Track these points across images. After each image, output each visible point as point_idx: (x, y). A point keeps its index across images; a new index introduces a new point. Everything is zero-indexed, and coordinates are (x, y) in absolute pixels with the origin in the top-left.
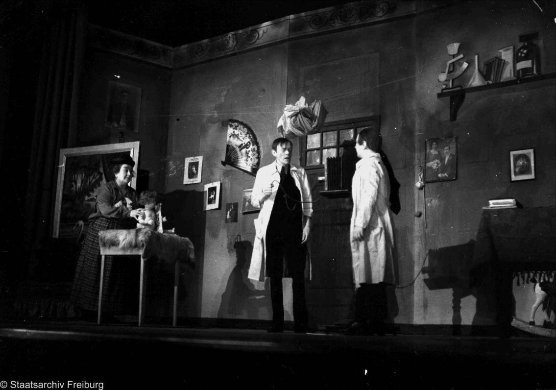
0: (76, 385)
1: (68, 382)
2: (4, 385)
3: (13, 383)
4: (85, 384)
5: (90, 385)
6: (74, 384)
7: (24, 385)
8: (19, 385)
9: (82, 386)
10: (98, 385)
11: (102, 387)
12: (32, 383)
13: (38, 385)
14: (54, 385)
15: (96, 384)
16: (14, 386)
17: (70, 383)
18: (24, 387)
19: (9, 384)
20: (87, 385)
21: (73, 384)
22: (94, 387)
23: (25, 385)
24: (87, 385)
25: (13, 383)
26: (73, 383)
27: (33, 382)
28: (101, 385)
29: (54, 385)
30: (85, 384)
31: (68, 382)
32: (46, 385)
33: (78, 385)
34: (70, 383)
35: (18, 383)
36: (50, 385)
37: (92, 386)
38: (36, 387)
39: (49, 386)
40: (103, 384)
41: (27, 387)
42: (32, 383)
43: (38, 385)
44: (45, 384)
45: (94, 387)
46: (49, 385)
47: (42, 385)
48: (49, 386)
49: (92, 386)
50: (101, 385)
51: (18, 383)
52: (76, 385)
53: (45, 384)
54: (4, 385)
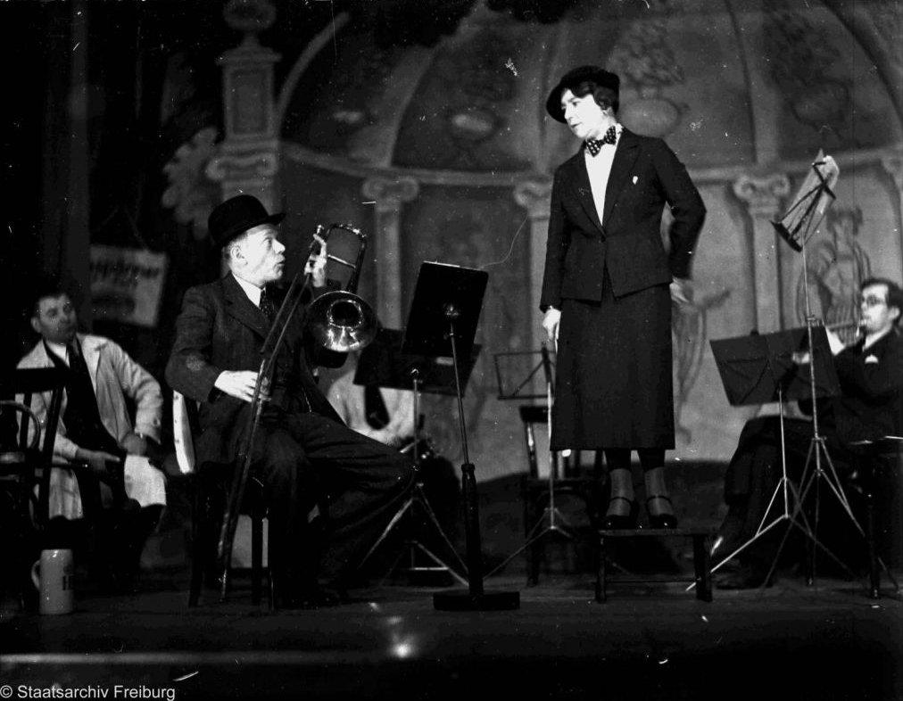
0: (128, 692)
3: (22, 689)
4: (144, 692)
5: (152, 693)
6: (126, 691)
8: (33, 693)
9: (138, 694)
10: (165, 692)
11: (173, 696)
12: (53, 689)
13: (64, 693)
14: (92, 692)
15: (163, 690)
16: (23, 694)
17: (118, 689)
19: (16, 691)
20: (147, 693)
21: (124, 691)
22: (158, 696)
23: (42, 693)
24: (147, 693)
25: (22, 689)
28: (171, 693)
29: (92, 692)
30: (144, 690)
32: (78, 692)
33: (133, 693)
34: (118, 689)
35: (30, 689)
36: (84, 693)
37: (156, 694)
38: (60, 695)
39: (83, 695)
40: (173, 690)
41: (46, 695)
43: (64, 693)
44: (76, 691)
45: (158, 696)
46: (84, 693)
47: (71, 693)
48: (83, 695)
49: (156, 694)
50: (171, 693)
51: (30, 689)
52: (128, 692)
53: (76, 691)
54: (6, 692)
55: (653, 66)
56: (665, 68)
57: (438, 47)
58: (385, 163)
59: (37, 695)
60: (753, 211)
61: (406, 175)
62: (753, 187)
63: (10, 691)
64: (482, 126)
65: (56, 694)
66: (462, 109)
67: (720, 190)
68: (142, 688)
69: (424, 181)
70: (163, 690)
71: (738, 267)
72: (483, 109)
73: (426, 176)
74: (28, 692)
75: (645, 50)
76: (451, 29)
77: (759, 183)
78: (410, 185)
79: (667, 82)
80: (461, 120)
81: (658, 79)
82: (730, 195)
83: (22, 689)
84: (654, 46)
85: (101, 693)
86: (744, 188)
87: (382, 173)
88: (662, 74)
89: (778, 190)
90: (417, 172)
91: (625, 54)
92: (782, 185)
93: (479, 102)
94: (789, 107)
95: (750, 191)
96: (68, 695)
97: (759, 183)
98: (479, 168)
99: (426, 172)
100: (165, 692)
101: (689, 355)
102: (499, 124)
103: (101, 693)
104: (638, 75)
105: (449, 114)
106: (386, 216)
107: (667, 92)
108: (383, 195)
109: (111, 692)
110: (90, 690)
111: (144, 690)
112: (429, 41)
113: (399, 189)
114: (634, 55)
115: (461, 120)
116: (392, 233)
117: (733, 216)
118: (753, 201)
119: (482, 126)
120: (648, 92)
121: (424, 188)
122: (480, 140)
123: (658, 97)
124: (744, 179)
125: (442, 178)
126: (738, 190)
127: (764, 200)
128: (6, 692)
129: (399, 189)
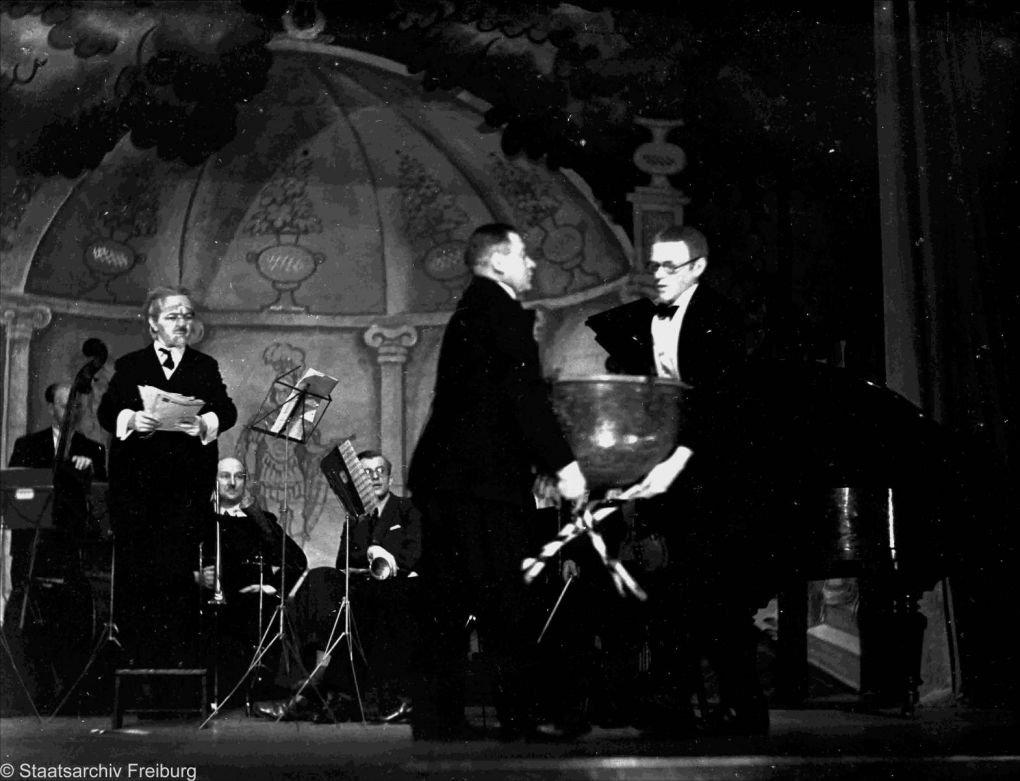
55: (294, 215)
56: (302, 217)
57: (79, 180)
58: (20, 290)
60: (381, 359)
61: (37, 303)
62: (384, 338)
64: (122, 260)
66: (101, 241)
67: (354, 334)
69: (60, 310)
71: (364, 412)
72: (124, 243)
73: (61, 306)
75: (285, 201)
76: (94, 164)
77: (388, 333)
78: (44, 316)
79: (306, 232)
80: (99, 253)
81: (297, 227)
82: (361, 343)
84: (294, 196)
86: (376, 336)
87: (13, 298)
88: (302, 224)
89: (406, 342)
90: (52, 300)
91: (266, 201)
92: (408, 335)
93: (120, 235)
94: (420, 263)
95: (380, 340)
97: (387, 333)
98: (115, 301)
99: (64, 302)
101: (314, 492)
102: (137, 259)
104: (278, 223)
105: (87, 245)
106: (13, 342)
107: (303, 240)
108: (15, 321)
112: (72, 174)
113: (31, 315)
114: (274, 201)
115: (99, 253)
116: (22, 359)
117: (361, 361)
118: (383, 350)
119: (122, 260)
120: (285, 238)
121: (55, 315)
122: (120, 273)
123: (296, 245)
124: (374, 329)
125: (77, 308)
126: (368, 337)
127: (393, 349)
129: (31, 315)
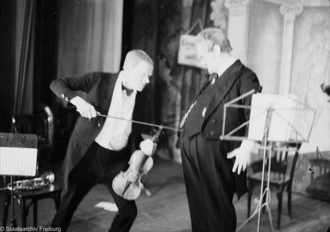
0: (44, 229)
1: (40, 227)
2: (2, 229)
3: (8, 228)
5: (53, 229)
6: (44, 228)
7: (14, 229)
8: (11, 229)
10: (57, 229)
11: (60, 230)
12: (19, 228)
14: (32, 229)
15: (57, 228)
16: (8, 230)
17: (41, 228)
18: (14, 230)
19: (5, 229)
20: (51, 229)
21: (43, 229)
22: (55, 230)
23: (15, 229)
26: (43, 228)
27: (20, 227)
28: (59, 229)
29: (32, 229)
30: (50, 228)
31: (40, 227)
32: (27, 229)
34: (41, 228)
35: (10, 228)
36: (29, 229)
37: (54, 230)
38: (21, 230)
40: (60, 228)
41: (16, 230)
42: (19, 228)
43: (22, 229)
45: (55, 230)
46: (29, 229)
49: (54, 230)
52: (44, 229)
59: (13, 230)
63: (3, 229)
65: (19, 229)
68: (49, 228)
70: (57, 228)
74: (9, 228)
83: (8, 228)
85: (35, 229)
96: (24, 230)
100: (57, 229)
103: (35, 229)
109: (39, 229)
110: (31, 228)
111: (50, 228)
128: (2, 229)
